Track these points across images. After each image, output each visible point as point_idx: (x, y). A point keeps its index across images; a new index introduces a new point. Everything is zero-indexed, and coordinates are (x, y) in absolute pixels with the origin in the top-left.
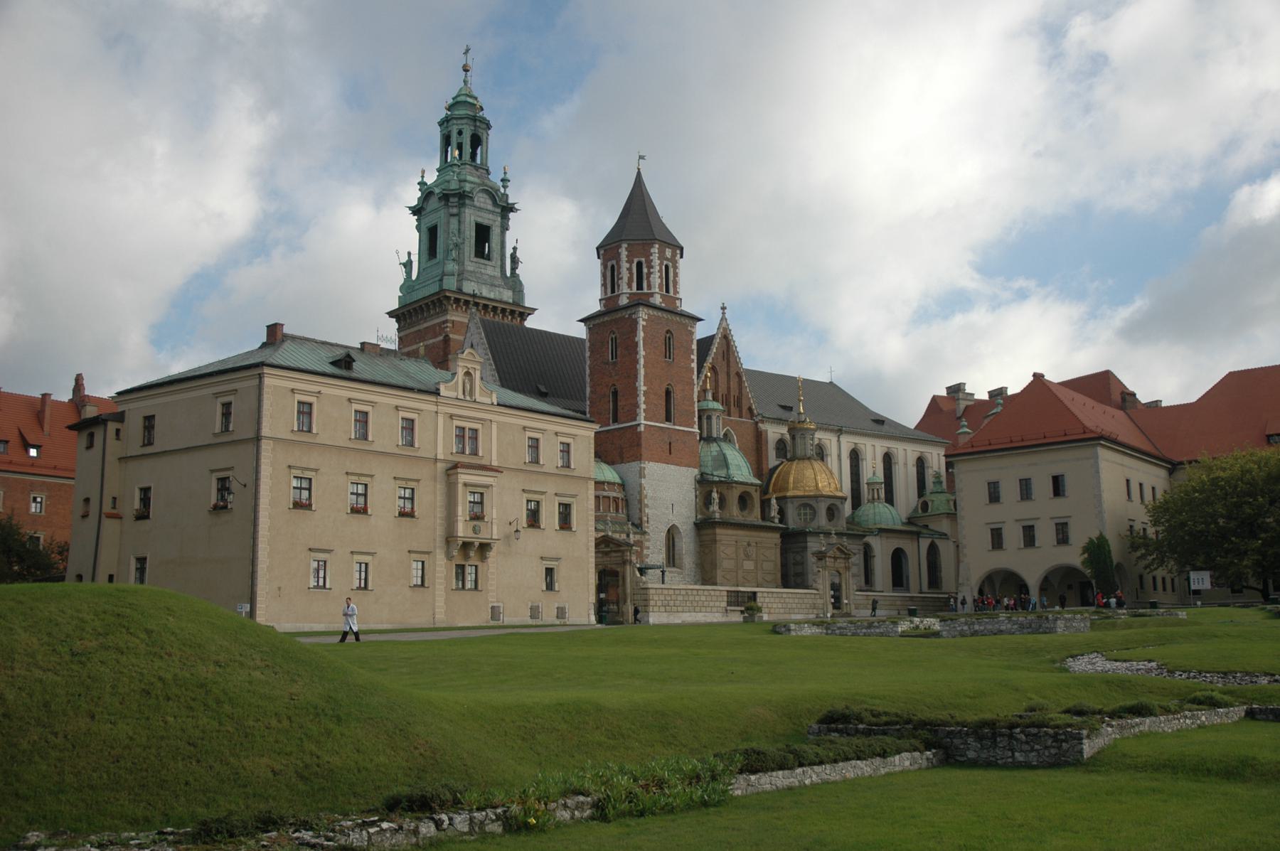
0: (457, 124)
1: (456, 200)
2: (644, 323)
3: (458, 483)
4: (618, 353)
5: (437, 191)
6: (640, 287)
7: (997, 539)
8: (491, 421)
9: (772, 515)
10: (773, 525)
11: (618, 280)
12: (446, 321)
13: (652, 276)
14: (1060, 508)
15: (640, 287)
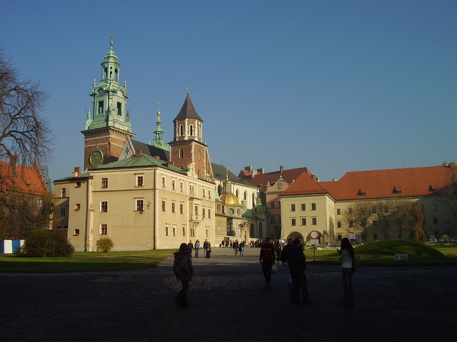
0: (110, 65)
1: (112, 93)
2: (194, 147)
3: (193, 203)
4: (184, 156)
5: (104, 89)
6: (191, 134)
7: (294, 222)
8: (196, 184)
9: (225, 212)
10: (225, 215)
11: (184, 132)
12: (110, 137)
13: (195, 131)
14: (314, 213)
15: (191, 134)
